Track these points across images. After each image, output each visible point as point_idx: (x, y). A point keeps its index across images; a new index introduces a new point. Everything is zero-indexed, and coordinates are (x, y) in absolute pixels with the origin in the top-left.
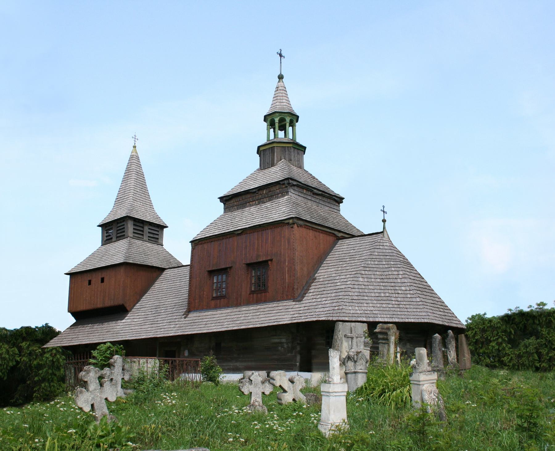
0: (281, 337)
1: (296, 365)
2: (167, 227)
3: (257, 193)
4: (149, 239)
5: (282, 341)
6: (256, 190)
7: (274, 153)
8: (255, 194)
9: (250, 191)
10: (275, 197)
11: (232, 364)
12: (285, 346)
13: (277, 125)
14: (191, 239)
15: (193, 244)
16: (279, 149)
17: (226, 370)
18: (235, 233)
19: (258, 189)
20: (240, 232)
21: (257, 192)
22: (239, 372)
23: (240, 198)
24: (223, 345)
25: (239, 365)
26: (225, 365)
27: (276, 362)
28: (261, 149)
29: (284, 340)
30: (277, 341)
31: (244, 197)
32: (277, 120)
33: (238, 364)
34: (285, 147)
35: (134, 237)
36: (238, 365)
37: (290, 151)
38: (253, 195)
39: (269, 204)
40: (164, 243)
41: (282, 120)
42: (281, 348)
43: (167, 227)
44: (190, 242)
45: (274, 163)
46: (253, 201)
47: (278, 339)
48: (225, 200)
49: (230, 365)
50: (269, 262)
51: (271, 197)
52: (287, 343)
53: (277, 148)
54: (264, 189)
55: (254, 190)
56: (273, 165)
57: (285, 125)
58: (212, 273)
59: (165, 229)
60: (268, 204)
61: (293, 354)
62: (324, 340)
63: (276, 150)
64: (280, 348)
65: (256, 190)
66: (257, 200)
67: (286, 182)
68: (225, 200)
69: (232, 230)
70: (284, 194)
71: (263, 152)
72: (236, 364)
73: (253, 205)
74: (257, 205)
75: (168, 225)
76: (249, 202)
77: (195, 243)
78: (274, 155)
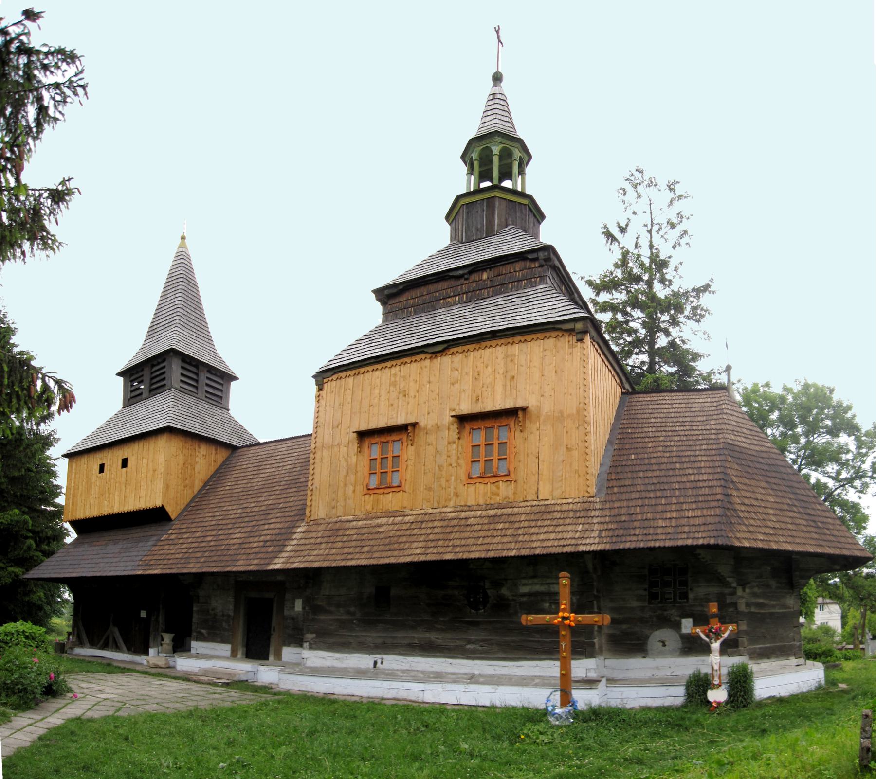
0: (549, 581)
1: (593, 644)
3: (466, 279)
5: (552, 590)
6: (466, 271)
7: (494, 210)
8: (462, 281)
9: (451, 274)
10: (512, 288)
11: (416, 636)
16: (504, 203)
18: (426, 350)
19: (470, 269)
20: (440, 348)
21: (466, 276)
22: (438, 654)
23: (424, 290)
24: (394, 592)
25: (438, 639)
26: (399, 635)
27: (538, 636)
28: (463, 201)
30: (538, 588)
31: (432, 288)
33: (434, 636)
34: (515, 202)
36: (433, 639)
37: (524, 211)
38: (452, 283)
39: (500, 299)
42: (550, 606)
45: (493, 230)
46: (456, 296)
47: (542, 584)
49: (414, 637)
50: (520, 414)
51: (500, 288)
53: (500, 204)
54: (484, 270)
55: (461, 272)
56: (490, 233)
57: (510, 166)
58: (363, 435)
60: (499, 300)
63: (497, 204)
64: (547, 605)
65: (466, 271)
66: (466, 293)
69: (419, 344)
70: (536, 282)
71: (467, 208)
72: (427, 635)
73: (455, 304)
74: (465, 303)
76: (444, 299)
78: (493, 214)
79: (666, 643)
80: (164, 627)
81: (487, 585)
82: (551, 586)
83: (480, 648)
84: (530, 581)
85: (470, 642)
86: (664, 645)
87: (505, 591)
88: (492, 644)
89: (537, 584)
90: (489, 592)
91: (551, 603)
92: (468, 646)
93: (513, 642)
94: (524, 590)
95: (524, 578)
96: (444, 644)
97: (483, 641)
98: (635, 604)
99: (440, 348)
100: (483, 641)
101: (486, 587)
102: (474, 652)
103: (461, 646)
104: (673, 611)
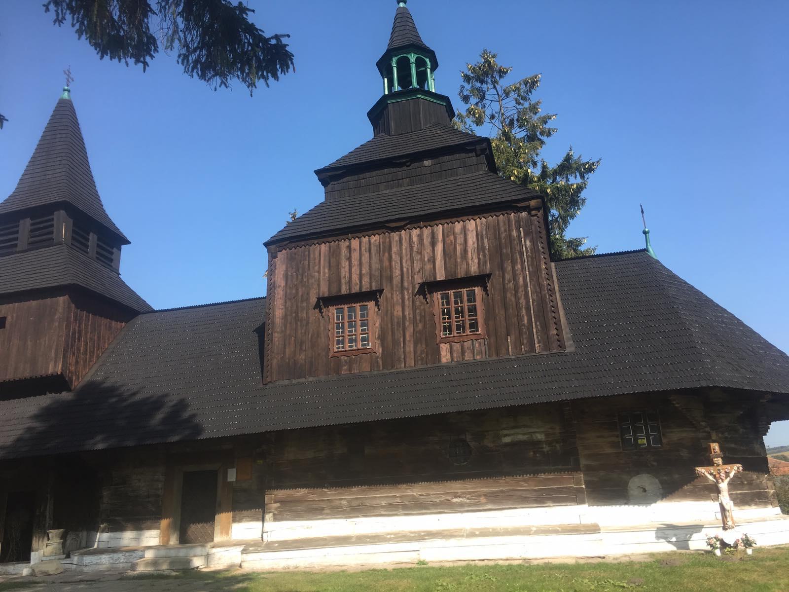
2: (128, 242)
4: (97, 258)
11: (398, 495)
12: (546, 448)
13: (413, 67)
14: (267, 238)
15: (273, 247)
17: (383, 507)
18: (387, 225)
20: (402, 223)
22: (424, 511)
25: (422, 495)
27: (526, 485)
29: (540, 437)
30: (521, 437)
32: (413, 58)
35: (72, 246)
40: (122, 270)
41: (420, 63)
43: (128, 242)
44: (266, 244)
47: (524, 434)
48: (327, 176)
49: (395, 497)
52: (549, 444)
59: (124, 247)
61: (570, 467)
62: (617, 437)
67: (478, 147)
68: (327, 176)
72: (409, 493)
75: (129, 239)
77: (275, 245)
79: (646, 489)
80: (51, 522)
81: (469, 437)
82: (533, 435)
83: (468, 501)
84: (512, 432)
85: (456, 496)
86: (645, 491)
87: (488, 443)
88: (480, 496)
89: (518, 434)
90: (472, 444)
91: (534, 452)
92: (455, 500)
93: (502, 492)
94: (507, 440)
95: (504, 429)
96: (429, 500)
97: (470, 493)
98: (609, 450)
99: (402, 223)
100: (470, 493)
101: (468, 440)
102: (461, 505)
103: (448, 500)
104: (649, 456)
